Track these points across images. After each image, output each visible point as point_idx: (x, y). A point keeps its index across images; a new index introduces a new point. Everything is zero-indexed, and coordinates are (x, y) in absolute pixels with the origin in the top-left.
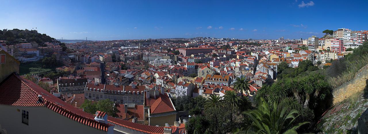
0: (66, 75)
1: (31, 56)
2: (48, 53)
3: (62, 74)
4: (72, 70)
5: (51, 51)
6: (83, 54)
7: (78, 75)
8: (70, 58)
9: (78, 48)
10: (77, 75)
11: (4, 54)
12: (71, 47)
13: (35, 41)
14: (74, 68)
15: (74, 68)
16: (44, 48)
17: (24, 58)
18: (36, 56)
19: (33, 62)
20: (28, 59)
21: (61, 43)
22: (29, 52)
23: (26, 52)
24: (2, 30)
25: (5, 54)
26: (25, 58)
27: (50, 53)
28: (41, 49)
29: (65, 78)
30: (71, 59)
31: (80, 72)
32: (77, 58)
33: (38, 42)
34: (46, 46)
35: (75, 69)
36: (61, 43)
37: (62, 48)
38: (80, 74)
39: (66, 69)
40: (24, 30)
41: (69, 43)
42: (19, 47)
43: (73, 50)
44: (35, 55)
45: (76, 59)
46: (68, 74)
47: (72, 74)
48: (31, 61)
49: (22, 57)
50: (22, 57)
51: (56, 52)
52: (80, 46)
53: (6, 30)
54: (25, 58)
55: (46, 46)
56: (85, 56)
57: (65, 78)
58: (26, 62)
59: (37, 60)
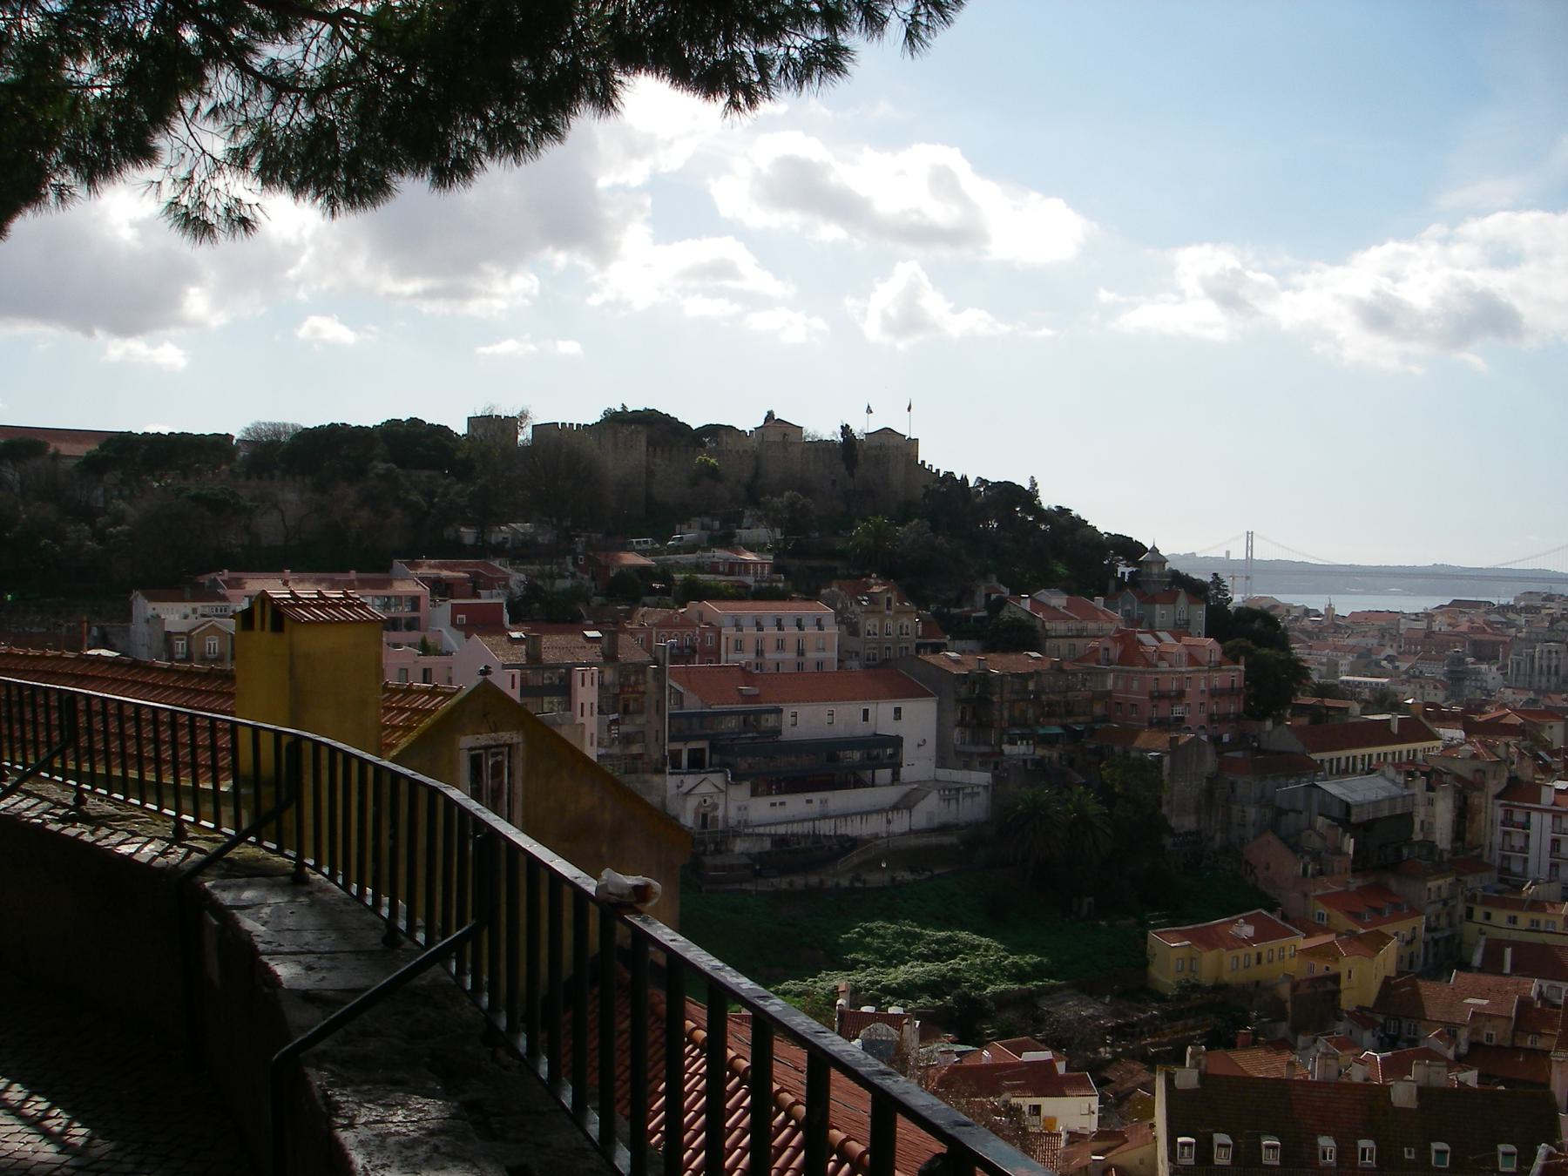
0: (1283, 1029)
1: (829, 766)
2: (1048, 741)
3: (1225, 1014)
4: (1364, 975)
5: (1098, 709)
6: (1527, 771)
7: (1438, 1045)
8: (1336, 813)
9: (1457, 676)
10: (1431, 1038)
11: (505, 736)
12: (1366, 661)
13: (887, 574)
14: (1390, 952)
15: (1390, 952)
16: (998, 664)
17: (746, 787)
18: (896, 766)
19: (850, 844)
20: (797, 804)
21: (1237, 599)
22: (807, 720)
23: (770, 721)
24: (460, 428)
25: (515, 737)
26: (754, 793)
27: (1074, 736)
28: (963, 678)
29: (1259, 1064)
30: (1362, 830)
31: (1471, 999)
32: (1443, 813)
33: (914, 578)
34: (1023, 636)
35: (1406, 965)
36: (1237, 599)
37: (1236, 673)
38: (1463, 1035)
39: (1288, 957)
40: (748, 421)
41: (1346, 606)
42: (683, 654)
43: (1384, 700)
44: (882, 752)
45: (1427, 827)
46: (1316, 1007)
47: (1362, 1016)
48: (826, 827)
49: (717, 778)
50: (708, 785)
51: (1162, 724)
52: (1485, 652)
53: (509, 425)
54: (754, 793)
55: (1023, 636)
56: (1547, 797)
57: (1259, 1064)
58: (767, 845)
59: (901, 823)
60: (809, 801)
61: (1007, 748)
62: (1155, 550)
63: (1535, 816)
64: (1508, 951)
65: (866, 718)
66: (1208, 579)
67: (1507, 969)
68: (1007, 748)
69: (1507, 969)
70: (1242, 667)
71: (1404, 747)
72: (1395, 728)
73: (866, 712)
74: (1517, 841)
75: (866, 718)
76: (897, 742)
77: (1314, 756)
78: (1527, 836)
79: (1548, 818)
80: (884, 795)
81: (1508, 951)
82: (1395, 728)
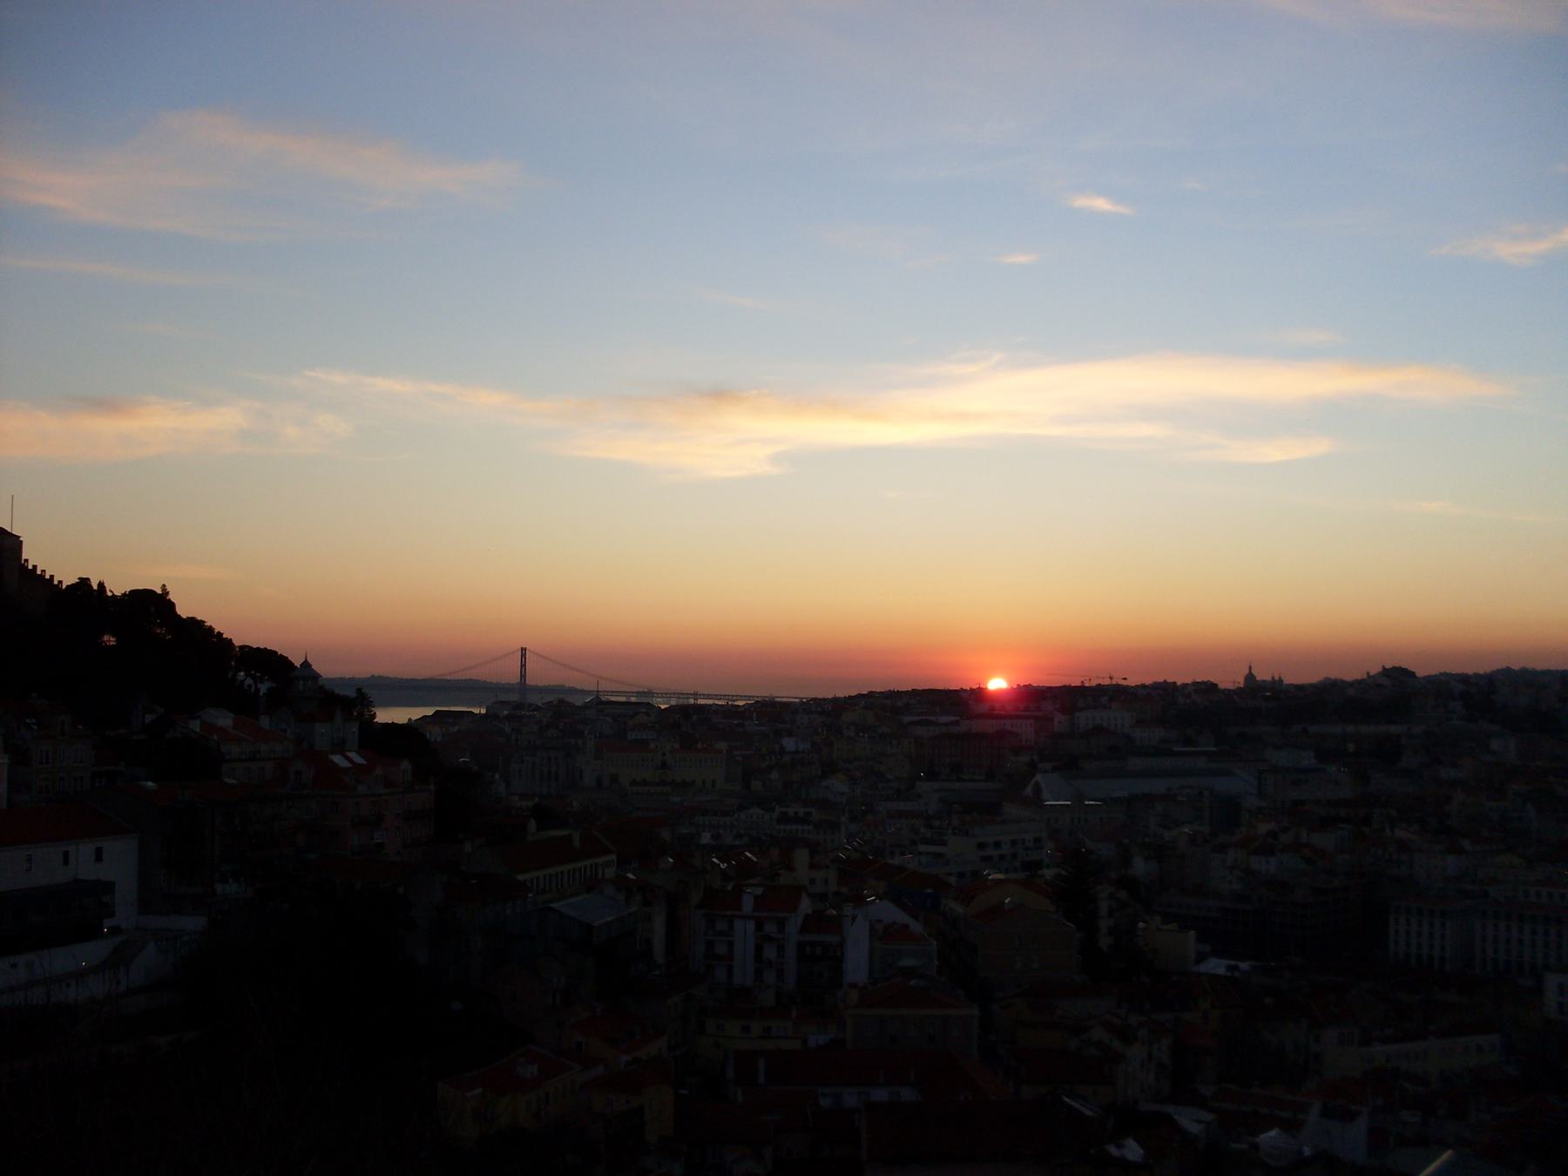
60: (14, 966)
61: (219, 887)
62: (306, 664)
63: (738, 924)
64: (761, 1063)
65: (66, 861)
66: (352, 694)
67: (762, 1079)
68: (219, 887)
69: (762, 1079)
70: (432, 787)
71: (588, 863)
72: (577, 843)
73: (66, 855)
74: (721, 949)
75: (66, 861)
76: (109, 887)
77: (521, 877)
78: (731, 944)
79: (751, 925)
80: (86, 954)
81: (761, 1063)
82: (577, 843)
